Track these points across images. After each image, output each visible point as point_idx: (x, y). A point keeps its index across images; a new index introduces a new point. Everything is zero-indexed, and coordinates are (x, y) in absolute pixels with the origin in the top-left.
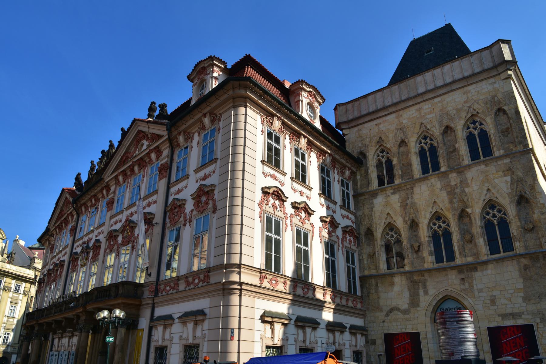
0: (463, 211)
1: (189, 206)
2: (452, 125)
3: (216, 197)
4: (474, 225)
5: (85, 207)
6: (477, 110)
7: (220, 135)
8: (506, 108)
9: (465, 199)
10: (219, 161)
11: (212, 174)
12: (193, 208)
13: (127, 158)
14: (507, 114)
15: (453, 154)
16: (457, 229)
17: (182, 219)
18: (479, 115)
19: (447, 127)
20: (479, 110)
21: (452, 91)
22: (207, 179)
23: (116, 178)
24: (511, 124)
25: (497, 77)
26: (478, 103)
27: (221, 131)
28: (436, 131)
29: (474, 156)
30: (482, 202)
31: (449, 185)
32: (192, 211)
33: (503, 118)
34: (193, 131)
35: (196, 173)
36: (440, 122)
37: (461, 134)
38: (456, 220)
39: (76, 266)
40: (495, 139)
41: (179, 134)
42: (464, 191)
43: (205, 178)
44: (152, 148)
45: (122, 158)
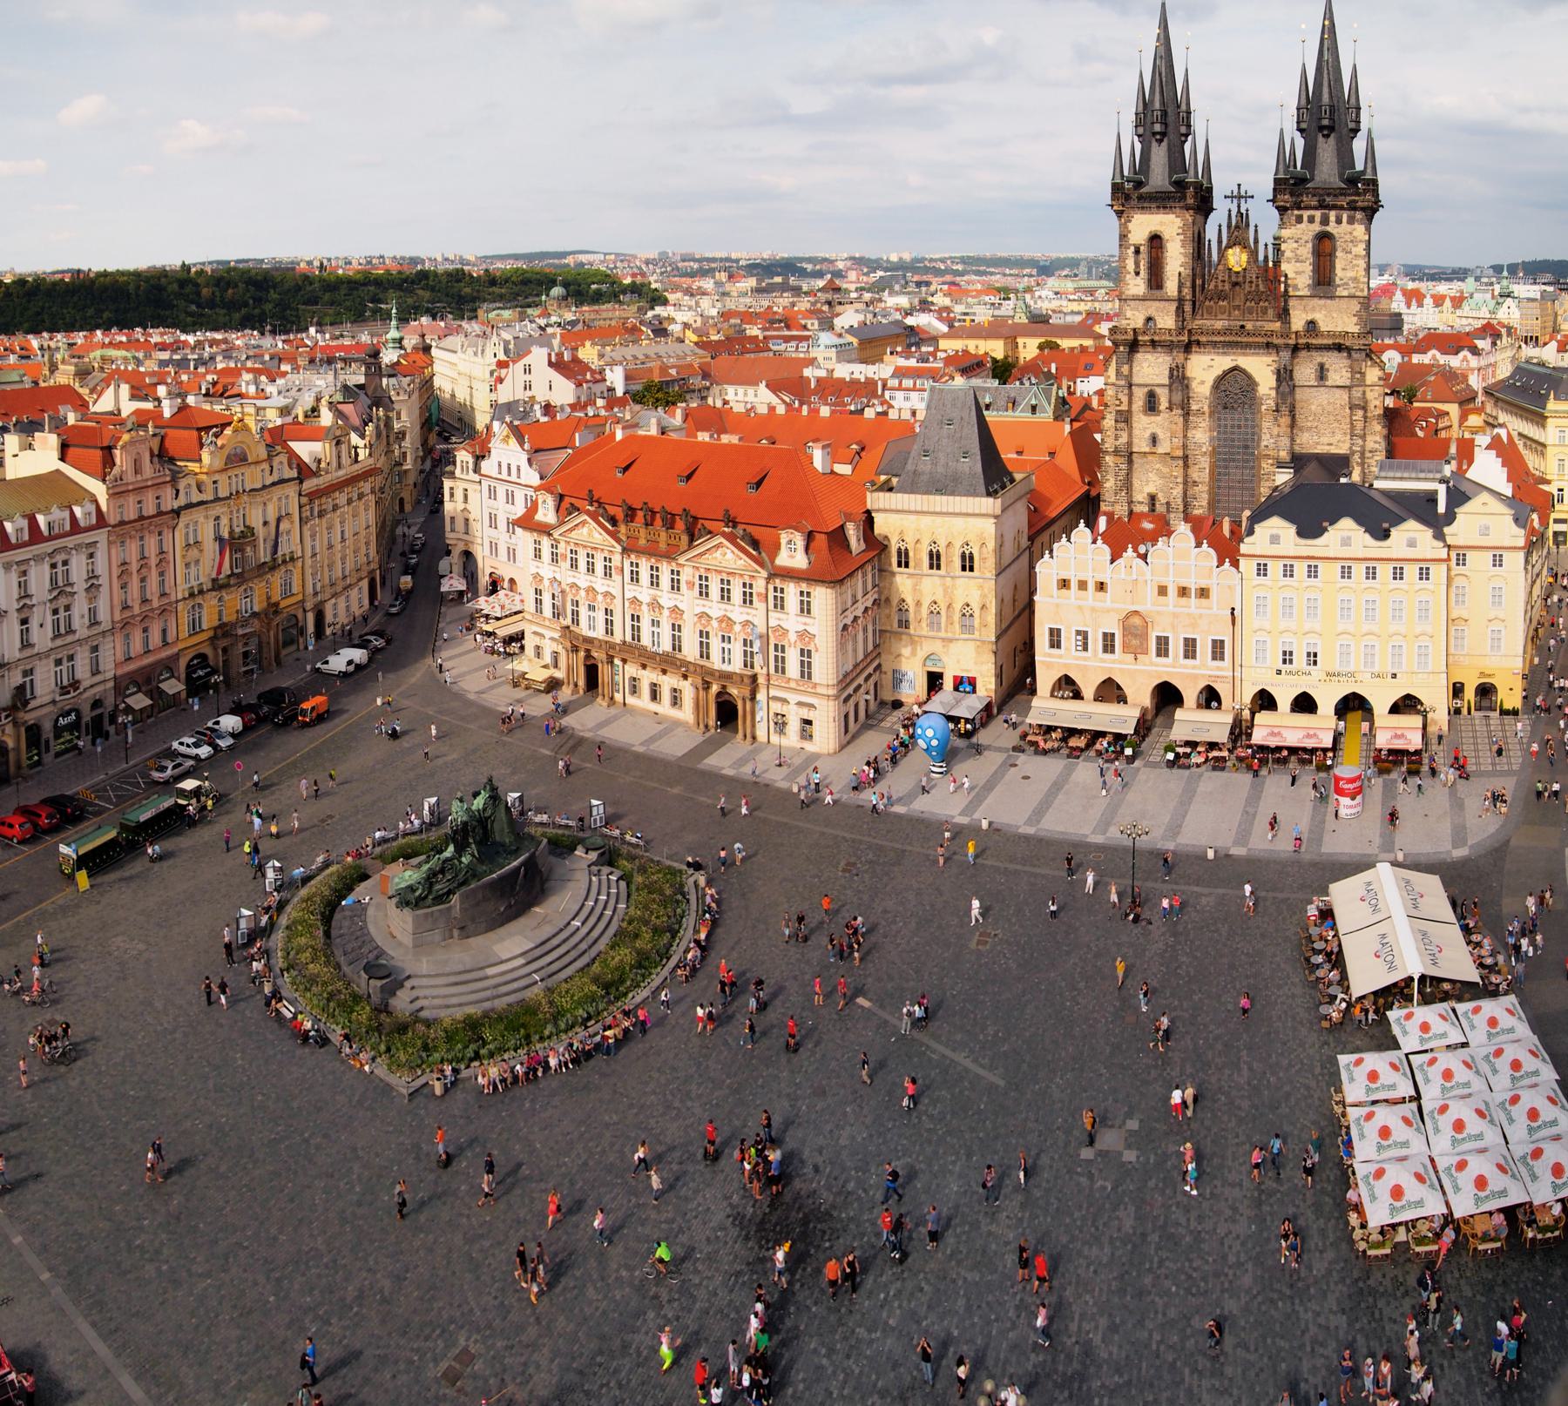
1: (792, 637)
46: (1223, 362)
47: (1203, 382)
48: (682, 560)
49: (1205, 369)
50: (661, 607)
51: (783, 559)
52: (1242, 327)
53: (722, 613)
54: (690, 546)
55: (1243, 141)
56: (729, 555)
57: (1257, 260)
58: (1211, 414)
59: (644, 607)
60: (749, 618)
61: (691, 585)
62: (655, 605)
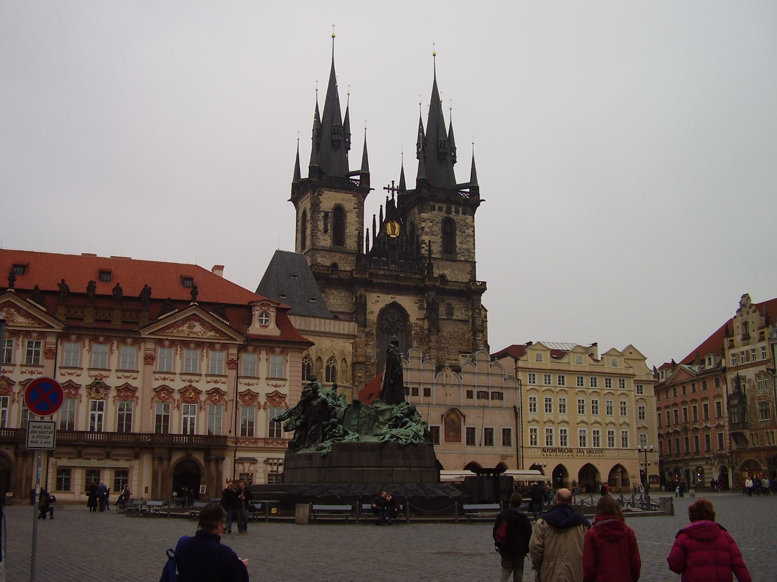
1: (262, 399)
2: (322, 357)
3: (287, 401)
5: (77, 337)
7: (288, 365)
8: (347, 359)
10: (288, 380)
11: (282, 386)
12: (266, 401)
13: (173, 326)
14: (347, 363)
17: (256, 403)
19: (319, 357)
21: (326, 336)
27: (288, 362)
28: (314, 358)
29: (327, 380)
32: (266, 403)
33: (344, 364)
36: (316, 353)
39: (77, 394)
41: (251, 345)
43: (276, 386)
45: (169, 325)
46: (386, 299)
47: (372, 312)
49: (377, 302)
50: (107, 388)
51: (255, 329)
52: (397, 275)
53: (187, 384)
54: (154, 321)
55: (388, 159)
56: (198, 328)
57: (405, 232)
58: (377, 336)
59: (83, 392)
61: (149, 359)
62: (98, 386)
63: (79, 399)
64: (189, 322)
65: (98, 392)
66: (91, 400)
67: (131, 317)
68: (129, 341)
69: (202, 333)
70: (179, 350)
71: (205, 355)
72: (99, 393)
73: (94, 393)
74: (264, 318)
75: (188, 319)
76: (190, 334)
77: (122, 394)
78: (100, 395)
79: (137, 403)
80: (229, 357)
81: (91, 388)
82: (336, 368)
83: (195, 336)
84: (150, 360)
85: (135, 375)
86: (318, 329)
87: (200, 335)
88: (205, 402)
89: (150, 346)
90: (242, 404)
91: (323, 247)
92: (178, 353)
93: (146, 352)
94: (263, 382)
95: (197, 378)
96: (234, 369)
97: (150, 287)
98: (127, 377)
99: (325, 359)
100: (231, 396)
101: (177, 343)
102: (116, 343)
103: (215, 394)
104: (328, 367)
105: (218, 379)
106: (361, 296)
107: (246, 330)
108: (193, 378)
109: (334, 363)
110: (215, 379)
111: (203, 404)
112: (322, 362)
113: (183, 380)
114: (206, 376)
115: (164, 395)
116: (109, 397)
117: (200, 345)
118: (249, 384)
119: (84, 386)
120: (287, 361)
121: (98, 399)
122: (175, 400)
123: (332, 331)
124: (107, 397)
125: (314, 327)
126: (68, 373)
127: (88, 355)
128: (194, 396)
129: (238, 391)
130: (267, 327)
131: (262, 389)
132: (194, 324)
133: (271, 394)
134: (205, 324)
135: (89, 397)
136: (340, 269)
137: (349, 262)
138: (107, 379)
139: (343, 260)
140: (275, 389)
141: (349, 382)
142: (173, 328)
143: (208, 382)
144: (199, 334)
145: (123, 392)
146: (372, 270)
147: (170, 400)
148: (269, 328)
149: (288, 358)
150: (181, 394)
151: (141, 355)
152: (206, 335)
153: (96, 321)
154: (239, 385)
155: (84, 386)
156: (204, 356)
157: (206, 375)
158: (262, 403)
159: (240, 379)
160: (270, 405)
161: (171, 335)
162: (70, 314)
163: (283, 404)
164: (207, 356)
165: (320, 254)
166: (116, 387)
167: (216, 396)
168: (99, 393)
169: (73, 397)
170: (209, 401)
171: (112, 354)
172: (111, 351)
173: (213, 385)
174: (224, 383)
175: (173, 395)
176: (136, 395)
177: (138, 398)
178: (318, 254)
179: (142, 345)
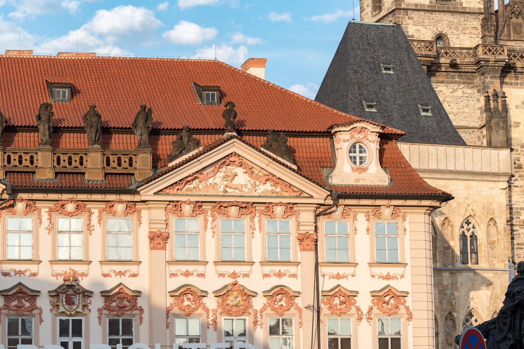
0: (450, 313)
1: (364, 302)
2: (451, 219)
4: (457, 330)
6: (475, 212)
7: (407, 238)
9: (453, 303)
10: (408, 267)
11: (399, 277)
12: (371, 305)
14: (497, 227)
15: (448, 251)
16: (443, 331)
17: (353, 310)
18: (476, 218)
20: (477, 212)
22: (391, 280)
23: (177, 205)
24: (498, 239)
25: (496, 183)
26: (477, 204)
30: (466, 309)
31: (441, 284)
32: (371, 309)
33: (493, 229)
34: (356, 210)
35: (370, 266)
37: (457, 233)
38: (443, 321)
39: (34, 307)
40: (485, 250)
42: (453, 294)
44: (285, 201)
48: (147, 193)
51: (344, 174)
53: (229, 281)
56: (242, 178)
59: (44, 303)
60: (285, 281)
61: (159, 240)
63: (37, 316)
64: (224, 169)
65: (70, 302)
66: (58, 318)
67: (119, 164)
68: (120, 208)
69: (249, 186)
70: (210, 219)
71: (257, 226)
72: (73, 303)
73: (63, 306)
74: (358, 155)
75: (224, 162)
76: (227, 189)
77: (114, 304)
78: (74, 307)
79: (141, 318)
80: (301, 228)
81: (58, 295)
82: (479, 237)
83: (237, 192)
84: (159, 240)
85: (133, 269)
86: (442, 167)
87: (246, 190)
88: (262, 312)
89: (159, 214)
90: (329, 312)
91: (416, 5)
92: (209, 225)
93: (152, 226)
94: (363, 269)
95: (245, 269)
96: (310, 250)
97: (150, 110)
98: (121, 273)
99: (457, 220)
100: (307, 298)
101: (205, 207)
102: (96, 212)
103: (279, 297)
104: (463, 237)
105: (283, 269)
106: (496, 95)
107: (327, 177)
108: (239, 269)
109: (474, 227)
110: (277, 269)
111: (258, 315)
112: (452, 226)
113: (222, 275)
114: (262, 265)
115: (189, 303)
116: (90, 310)
117: (246, 207)
118: (338, 277)
119: (44, 292)
120: (405, 230)
121: (71, 315)
122: (207, 311)
123: (469, 169)
124: (86, 311)
125: (435, 163)
126: (15, 271)
127: (49, 237)
128: (242, 303)
129: (320, 290)
130: (365, 170)
131: (363, 283)
132: (234, 171)
133: (380, 291)
134: (252, 170)
135: (54, 312)
136: (452, 45)
137: (468, 32)
138: (84, 277)
139: (457, 28)
140: (385, 283)
141: (503, 261)
142: (197, 181)
143: (266, 276)
144: (244, 189)
145: (115, 301)
146: (513, 43)
147: (200, 311)
148: (368, 171)
149: (407, 224)
150: (220, 300)
151: (144, 232)
152: (256, 190)
153: (57, 174)
154: (321, 279)
155: (44, 292)
156: (254, 229)
157: (262, 263)
158: (365, 310)
159: (322, 268)
160: (378, 312)
161: (194, 193)
162: (12, 165)
163: (402, 310)
164: (260, 228)
165: (412, 18)
166: (101, 292)
167: (281, 300)
168: (73, 303)
169: (26, 313)
170: (269, 311)
171: (91, 234)
172: (89, 227)
173: (274, 281)
174: (294, 276)
175: (204, 300)
176: (139, 306)
177: (141, 310)
178: (409, 18)
179: (145, 213)
